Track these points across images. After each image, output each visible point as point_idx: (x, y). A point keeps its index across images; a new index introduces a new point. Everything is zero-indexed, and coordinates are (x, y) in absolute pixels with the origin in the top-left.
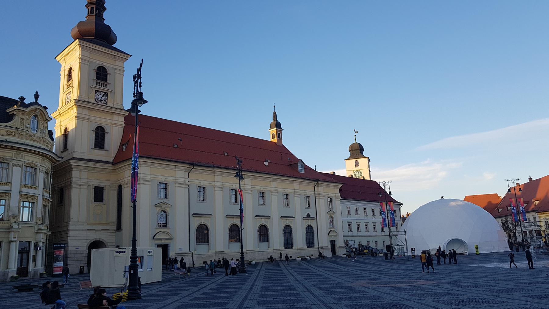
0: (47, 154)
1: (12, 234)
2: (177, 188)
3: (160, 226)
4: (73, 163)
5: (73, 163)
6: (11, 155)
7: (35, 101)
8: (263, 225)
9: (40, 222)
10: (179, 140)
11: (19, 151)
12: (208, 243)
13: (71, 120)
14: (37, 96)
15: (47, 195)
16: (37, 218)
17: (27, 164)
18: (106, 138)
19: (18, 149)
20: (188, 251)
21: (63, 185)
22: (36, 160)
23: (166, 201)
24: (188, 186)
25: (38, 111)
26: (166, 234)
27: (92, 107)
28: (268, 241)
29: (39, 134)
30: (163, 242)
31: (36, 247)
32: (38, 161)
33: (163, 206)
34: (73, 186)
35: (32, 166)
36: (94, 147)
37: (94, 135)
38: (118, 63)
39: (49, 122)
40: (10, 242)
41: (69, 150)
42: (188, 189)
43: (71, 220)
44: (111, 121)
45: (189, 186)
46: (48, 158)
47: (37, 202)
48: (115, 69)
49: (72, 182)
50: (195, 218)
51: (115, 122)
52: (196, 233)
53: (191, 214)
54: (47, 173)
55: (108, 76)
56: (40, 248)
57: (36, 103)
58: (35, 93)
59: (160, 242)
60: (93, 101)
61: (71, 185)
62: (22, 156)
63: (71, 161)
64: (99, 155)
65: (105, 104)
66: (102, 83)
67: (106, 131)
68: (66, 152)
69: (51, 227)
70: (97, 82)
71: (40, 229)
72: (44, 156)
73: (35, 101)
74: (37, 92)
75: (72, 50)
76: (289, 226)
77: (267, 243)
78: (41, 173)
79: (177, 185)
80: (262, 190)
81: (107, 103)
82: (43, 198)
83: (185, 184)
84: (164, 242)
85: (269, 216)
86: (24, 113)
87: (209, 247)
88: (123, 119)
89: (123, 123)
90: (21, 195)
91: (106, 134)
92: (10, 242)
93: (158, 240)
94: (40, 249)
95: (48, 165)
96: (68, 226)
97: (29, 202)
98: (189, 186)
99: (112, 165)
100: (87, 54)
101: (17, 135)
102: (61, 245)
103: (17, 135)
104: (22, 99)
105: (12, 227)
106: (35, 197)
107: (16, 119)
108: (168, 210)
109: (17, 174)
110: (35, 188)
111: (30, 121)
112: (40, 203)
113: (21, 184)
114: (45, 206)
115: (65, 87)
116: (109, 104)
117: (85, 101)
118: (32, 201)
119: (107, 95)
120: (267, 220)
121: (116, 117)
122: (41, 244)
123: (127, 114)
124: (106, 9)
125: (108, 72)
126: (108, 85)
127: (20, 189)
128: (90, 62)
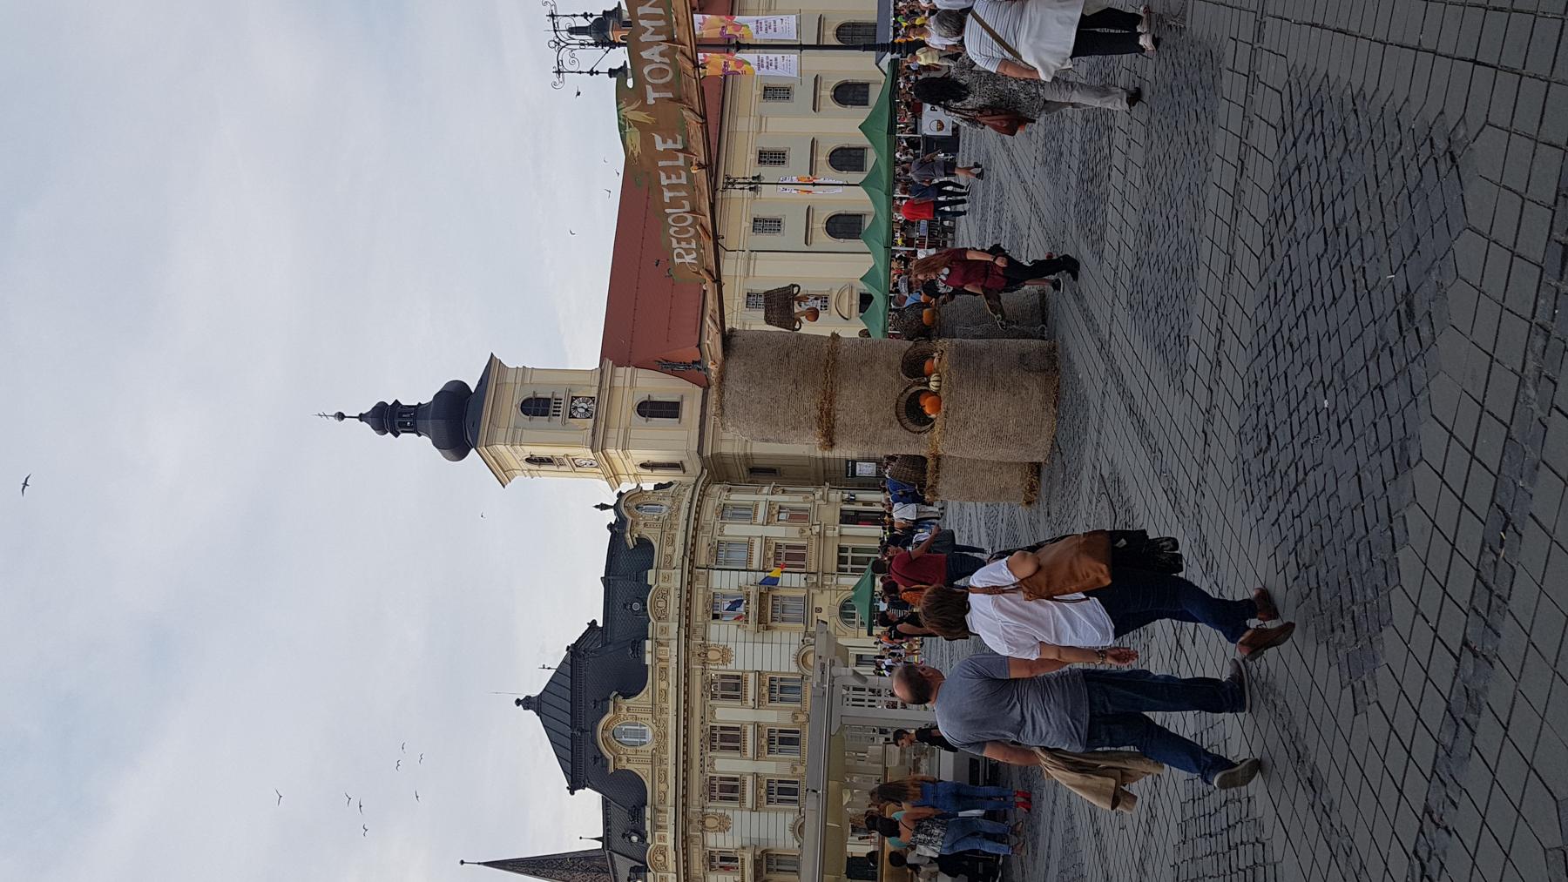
0: (701, 490)
1: (829, 533)
2: (756, 275)
3: (826, 306)
4: (708, 452)
5: (708, 452)
6: (705, 539)
7: (612, 510)
9: (812, 498)
10: (657, 265)
11: (699, 528)
13: (627, 457)
14: (603, 507)
15: (766, 489)
16: (804, 502)
17: (718, 517)
18: (659, 399)
19: (695, 529)
21: (744, 469)
22: (710, 506)
24: (753, 253)
25: (628, 504)
26: (842, 297)
27: (603, 424)
28: (869, 84)
29: (668, 502)
30: (854, 302)
31: (850, 501)
32: (711, 502)
34: (748, 451)
35: (720, 509)
36: (677, 420)
37: (655, 419)
38: (510, 379)
39: (644, 489)
40: (841, 535)
41: (681, 458)
43: (807, 453)
44: (627, 390)
45: (752, 251)
46: (705, 489)
47: (778, 502)
48: (523, 384)
49: (742, 453)
50: (814, 240)
51: (627, 384)
52: (842, 240)
53: (806, 248)
54: (730, 490)
55: (539, 396)
56: (852, 496)
57: (616, 507)
58: (598, 510)
59: (856, 308)
60: (591, 421)
61: (746, 455)
62: (706, 524)
63: (705, 455)
64: (691, 411)
65: (594, 401)
66: (555, 407)
67: (646, 399)
68: (687, 466)
69: (818, 483)
70: (554, 415)
71: (822, 498)
72: (703, 494)
73: (612, 510)
74: (597, 507)
75: (494, 457)
76: (838, 29)
77: (870, 85)
79: (751, 274)
80: (759, 92)
81: (591, 398)
82: (772, 494)
83: (749, 259)
84: (856, 301)
85: (816, 79)
86: (634, 523)
88: (621, 371)
89: (629, 369)
90: (768, 523)
91: (651, 399)
92: (841, 535)
94: (854, 496)
95: (715, 489)
96: (816, 458)
97: (779, 512)
98: (752, 251)
99: (709, 388)
100: (501, 433)
101: (673, 532)
102: (850, 465)
103: (673, 532)
104: (610, 527)
105: (819, 533)
106: (770, 504)
107: (647, 533)
109: (735, 530)
110: (757, 506)
111: (646, 515)
112: (779, 498)
113: (751, 524)
114: (784, 492)
115: (562, 468)
116: (594, 394)
117: (593, 435)
118: (777, 508)
119: (576, 398)
120: (823, 85)
121: (618, 382)
122: (846, 496)
123: (611, 362)
124: (396, 401)
125: (531, 396)
126: (557, 396)
127: (759, 524)
128: (515, 427)
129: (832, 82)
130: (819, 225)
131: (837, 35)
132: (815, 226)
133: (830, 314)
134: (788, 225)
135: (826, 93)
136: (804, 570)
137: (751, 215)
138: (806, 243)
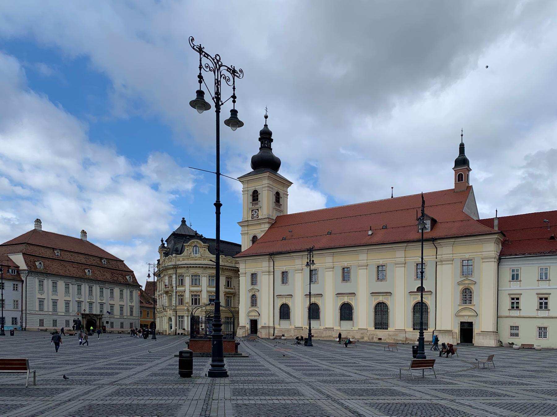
8: (346, 303)
12: (289, 320)
20: (272, 325)
22: (199, 271)
23: (255, 287)
24: (273, 273)
30: (253, 317)
33: (253, 291)
42: (273, 276)
77: (351, 321)
78: (203, 278)
82: (208, 292)
84: (253, 318)
85: (354, 293)
87: (291, 323)
93: (252, 316)
108: (257, 294)
113: (190, 286)
127: (189, 288)
129: (352, 302)
130: (284, 301)
131: (380, 303)
132: (284, 299)
133: (250, 308)
134: (284, 287)
135: (346, 299)
136: (177, 305)
137: (258, 272)
138: (276, 296)
